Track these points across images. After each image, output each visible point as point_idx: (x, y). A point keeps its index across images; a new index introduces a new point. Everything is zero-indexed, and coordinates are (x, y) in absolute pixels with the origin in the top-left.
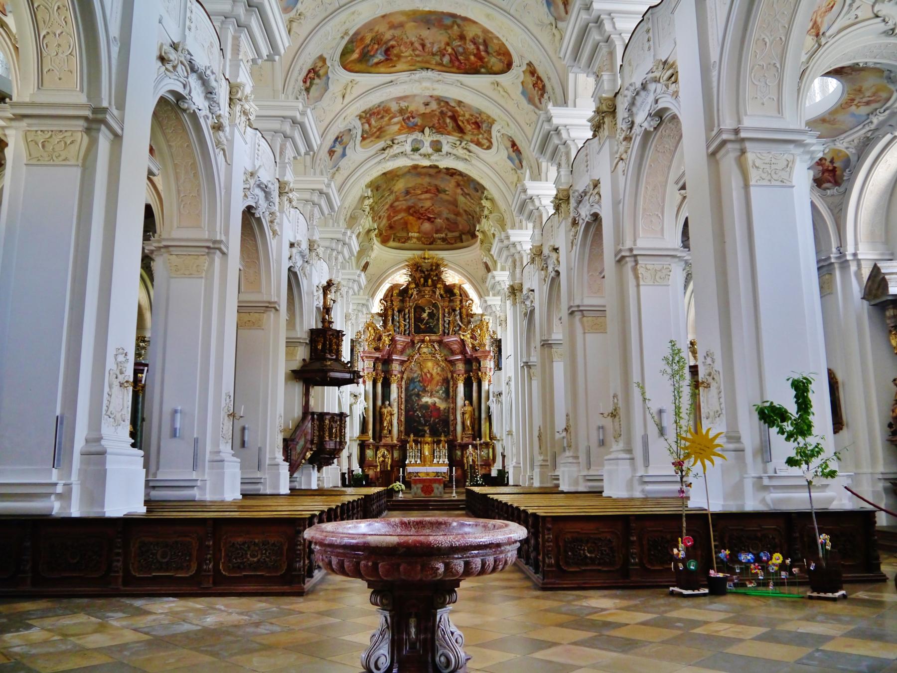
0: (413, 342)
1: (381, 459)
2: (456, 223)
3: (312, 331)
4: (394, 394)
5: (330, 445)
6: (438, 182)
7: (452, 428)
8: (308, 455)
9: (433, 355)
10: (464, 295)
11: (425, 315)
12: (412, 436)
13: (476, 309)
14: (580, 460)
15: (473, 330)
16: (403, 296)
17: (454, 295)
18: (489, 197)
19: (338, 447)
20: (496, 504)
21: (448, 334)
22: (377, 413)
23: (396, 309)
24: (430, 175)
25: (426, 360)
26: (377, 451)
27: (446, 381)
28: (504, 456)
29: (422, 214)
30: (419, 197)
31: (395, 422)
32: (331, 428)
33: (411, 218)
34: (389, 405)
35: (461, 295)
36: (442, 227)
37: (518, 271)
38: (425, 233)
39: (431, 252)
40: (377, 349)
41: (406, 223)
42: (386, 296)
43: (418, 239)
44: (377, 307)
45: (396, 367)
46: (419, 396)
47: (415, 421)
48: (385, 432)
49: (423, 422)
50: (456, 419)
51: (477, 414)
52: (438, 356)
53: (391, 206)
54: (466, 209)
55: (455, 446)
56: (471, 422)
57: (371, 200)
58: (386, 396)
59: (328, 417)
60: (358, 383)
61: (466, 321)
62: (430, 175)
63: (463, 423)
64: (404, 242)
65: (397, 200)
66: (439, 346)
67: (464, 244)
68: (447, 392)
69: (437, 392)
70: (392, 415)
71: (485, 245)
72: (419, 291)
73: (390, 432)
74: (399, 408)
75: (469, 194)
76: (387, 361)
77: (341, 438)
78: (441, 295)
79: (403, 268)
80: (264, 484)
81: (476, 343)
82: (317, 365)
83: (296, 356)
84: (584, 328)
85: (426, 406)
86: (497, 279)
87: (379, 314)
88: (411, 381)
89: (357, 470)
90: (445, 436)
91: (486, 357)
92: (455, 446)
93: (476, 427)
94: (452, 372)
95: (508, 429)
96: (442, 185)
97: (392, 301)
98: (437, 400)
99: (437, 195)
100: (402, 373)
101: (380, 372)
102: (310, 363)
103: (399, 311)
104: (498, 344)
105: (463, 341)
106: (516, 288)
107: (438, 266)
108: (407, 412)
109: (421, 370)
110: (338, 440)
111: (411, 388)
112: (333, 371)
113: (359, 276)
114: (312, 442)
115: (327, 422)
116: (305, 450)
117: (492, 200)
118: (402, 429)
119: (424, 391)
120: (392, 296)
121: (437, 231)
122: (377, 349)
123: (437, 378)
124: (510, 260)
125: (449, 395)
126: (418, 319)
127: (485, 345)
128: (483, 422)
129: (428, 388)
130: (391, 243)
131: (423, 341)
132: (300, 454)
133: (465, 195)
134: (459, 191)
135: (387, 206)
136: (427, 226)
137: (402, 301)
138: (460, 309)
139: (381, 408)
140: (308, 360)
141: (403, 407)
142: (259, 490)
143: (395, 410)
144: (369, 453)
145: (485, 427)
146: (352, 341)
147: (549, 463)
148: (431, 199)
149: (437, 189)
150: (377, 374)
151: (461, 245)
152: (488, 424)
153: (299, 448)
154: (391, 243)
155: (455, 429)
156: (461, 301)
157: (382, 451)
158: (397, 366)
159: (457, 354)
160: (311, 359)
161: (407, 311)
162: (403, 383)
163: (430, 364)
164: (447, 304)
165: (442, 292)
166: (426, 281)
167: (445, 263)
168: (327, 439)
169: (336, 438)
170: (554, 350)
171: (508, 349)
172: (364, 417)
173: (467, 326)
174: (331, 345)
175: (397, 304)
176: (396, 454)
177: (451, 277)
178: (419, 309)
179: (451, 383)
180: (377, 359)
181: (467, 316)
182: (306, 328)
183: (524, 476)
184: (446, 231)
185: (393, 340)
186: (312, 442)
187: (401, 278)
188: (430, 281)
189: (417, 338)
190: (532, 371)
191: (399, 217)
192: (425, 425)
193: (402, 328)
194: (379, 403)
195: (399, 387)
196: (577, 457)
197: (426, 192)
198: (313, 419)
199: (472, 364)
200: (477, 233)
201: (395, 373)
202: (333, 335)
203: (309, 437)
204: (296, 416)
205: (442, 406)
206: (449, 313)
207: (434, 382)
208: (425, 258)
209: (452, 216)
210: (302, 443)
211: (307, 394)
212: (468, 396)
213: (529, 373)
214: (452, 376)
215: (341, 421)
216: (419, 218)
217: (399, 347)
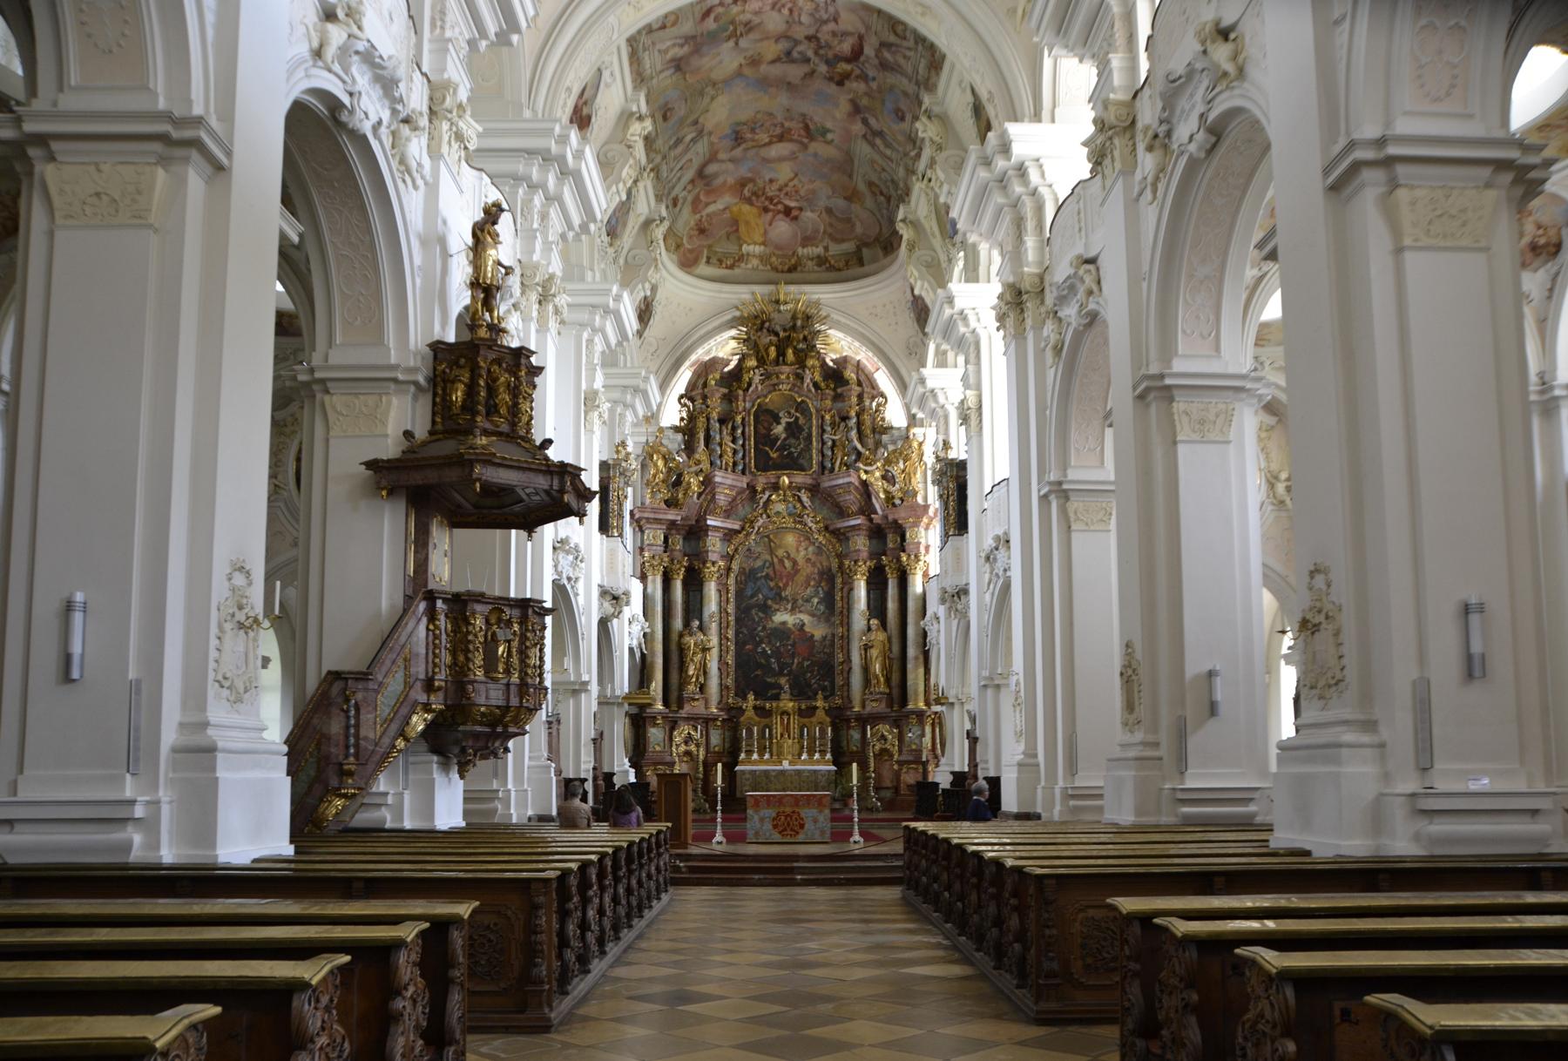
0: (752, 488)
1: (683, 748)
2: (849, 220)
3: (438, 348)
4: (712, 605)
5: (488, 696)
6: (804, 107)
7: (839, 681)
8: (418, 723)
9: (798, 518)
10: (867, 385)
11: (779, 430)
12: (751, 697)
13: (895, 414)
14: (1385, 733)
15: (888, 462)
16: (729, 386)
17: (847, 383)
18: (936, 109)
19: (514, 701)
20: (989, 872)
21: (832, 470)
22: (674, 647)
23: (715, 415)
24: (790, 86)
25: (781, 530)
26: (672, 729)
27: (827, 577)
28: (973, 739)
29: (771, 199)
30: (764, 152)
31: (713, 666)
32: (491, 643)
33: (746, 208)
34: (701, 628)
35: (860, 384)
36: (817, 231)
37: (1030, 242)
38: (778, 247)
39: (792, 288)
40: (671, 503)
41: (735, 222)
42: (691, 386)
43: (763, 259)
44: (672, 414)
45: (714, 545)
46: (766, 609)
47: (759, 666)
48: (691, 688)
49: (775, 666)
50: (848, 660)
51: (896, 648)
52: (809, 521)
53: (701, 174)
54: (874, 178)
55: (848, 721)
56: (883, 667)
57: (648, 125)
58: (693, 608)
59: (479, 608)
60: (581, 515)
61: (870, 442)
62: (790, 86)
63: (866, 669)
64: (731, 267)
65: (712, 158)
66: (811, 499)
67: (866, 269)
68: (829, 600)
69: (808, 601)
70: (705, 650)
71: (918, 253)
72: (767, 376)
73: (702, 688)
74: (722, 637)
75: (880, 134)
76: (695, 532)
77: (523, 675)
78: (816, 385)
79: (731, 324)
80: (150, 825)
81: (894, 489)
82: (448, 447)
83: (384, 424)
84: (1396, 230)
85: (782, 632)
86: (959, 304)
87: (676, 429)
88: (748, 576)
89: (624, 773)
90: (826, 698)
91: (919, 518)
92: (848, 721)
93: (895, 677)
94: (840, 556)
95: (986, 673)
96: (818, 115)
97: (705, 398)
98: (806, 618)
99: (805, 147)
100: (729, 558)
101: (678, 555)
102: (424, 444)
103: (722, 421)
104: (954, 478)
105: (865, 484)
106: (1026, 285)
107: (808, 318)
108: (739, 645)
109: (772, 552)
110: (515, 679)
111: (749, 592)
112: (489, 460)
113: (618, 298)
114: (429, 686)
115: (479, 622)
116: (405, 707)
117: (943, 120)
118: (730, 682)
119: (779, 598)
120: (705, 385)
121: (807, 241)
122: (671, 503)
123: (806, 570)
124: (1007, 219)
125: (834, 606)
126: (765, 439)
127: (915, 494)
128: (910, 666)
129: (787, 593)
130: (703, 268)
131: (776, 487)
132: (388, 721)
133: (872, 135)
134: (858, 128)
135: (690, 174)
136: (782, 229)
137: (729, 398)
138: (858, 415)
139: (681, 636)
140: (421, 433)
141: (731, 634)
142: (127, 847)
143: (714, 641)
144: (655, 734)
145: (915, 676)
146: (604, 466)
147: (1162, 752)
148: (792, 157)
149: (807, 128)
150: (672, 560)
151: (860, 270)
152: (921, 670)
153: (385, 702)
154: (703, 268)
155: (848, 684)
156: (860, 397)
157: (684, 729)
158: (718, 544)
159: (854, 514)
160: (431, 433)
161: (739, 419)
162: (731, 581)
163: (790, 539)
164: (828, 402)
165: (818, 378)
166: (781, 353)
167: (823, 313)
168: (480, 673)
169: (507, 672)
170: (1179, 406)
171: (995, 462)
172: (643, 655)
173: (874, 451)
174: (492, 391)
175: (716, 407)
176: (715, 738)
177: (838, 344)
178: (765, 416)
179: (839, 580)
180: (673, 523)
181: (874, 431)
182: (418, 339)
183: (1050, 789)
184: (827, 241)
185: (707, 482)
186: (429, 686)
187: (725, 347)
188: (790, 351)
189: (761, 481)
190: (1074, 505)
191: (719, 206)
192: (781, 674)
193: (728, 458)
194: (678, 623)
195: (723, 590)
196: (1370, 725)
197: (781, 138)
198: (432, 615)
199: (890, 539)
200: (902, 229)
201: (712, 557)
202: (498, 361)
203: (420, 670)
204: (384, 604)
205: (818, 631)
206: (833, 424)
207: (800, 578)
208: (777, 302)
209: (840, 203)
210: (395, 684)
211: (422, 542)
212: (877, 608)
213: (1063, 511)
214: (841, 566)
215: (523, 621)
216: (766, 210)
217: (722, 499)
